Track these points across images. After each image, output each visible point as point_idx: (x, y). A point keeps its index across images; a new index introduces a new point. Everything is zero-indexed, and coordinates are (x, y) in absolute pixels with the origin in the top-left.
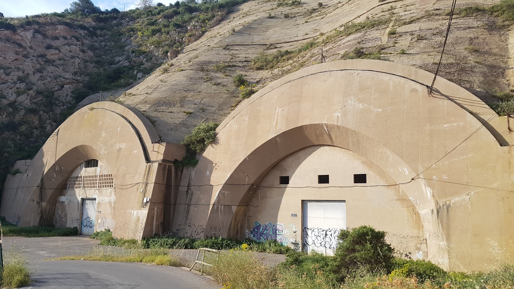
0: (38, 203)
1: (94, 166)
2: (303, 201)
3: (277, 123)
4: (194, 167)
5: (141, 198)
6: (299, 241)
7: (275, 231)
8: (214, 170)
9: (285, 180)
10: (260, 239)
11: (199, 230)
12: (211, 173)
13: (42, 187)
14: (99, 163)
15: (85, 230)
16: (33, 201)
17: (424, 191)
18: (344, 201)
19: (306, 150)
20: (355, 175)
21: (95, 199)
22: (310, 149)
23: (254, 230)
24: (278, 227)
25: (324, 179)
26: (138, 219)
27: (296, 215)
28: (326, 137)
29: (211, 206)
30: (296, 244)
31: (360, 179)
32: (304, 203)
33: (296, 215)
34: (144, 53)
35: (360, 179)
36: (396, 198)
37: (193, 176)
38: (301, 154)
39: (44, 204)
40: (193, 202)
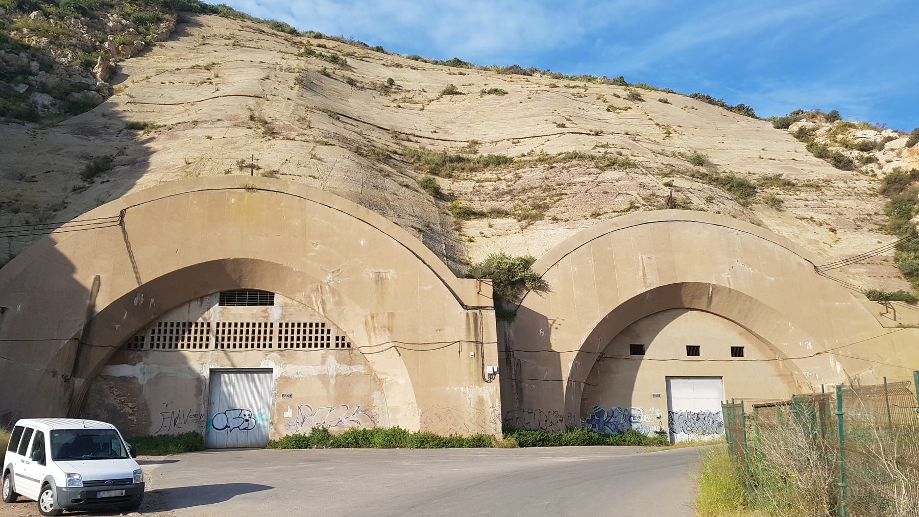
0: (66, 380)
1: (261, 304)
2: (668, 378)
3: (644, 274)
4: (510, 323)
5: (474, 366)
6: (666, 429)
7: (629, 418)
8: (553, 329)
9: (639, 350)
10: (604, 430)
11: (552, 418)
12: (548, 332)
13: (82, 342)
14: (277, 299)
15: (217, 437)
16: (55, 374)
17: (832, 364)
18: (721, 377)
19: (668, 313)
20: (699, 347)
21: (270, 371)
22: (674, 312)
23: (593, 417)
24: (633, 412)
25: (693, 351)
26: (481, 401)
27: (659, 396)
28: (705, 300)
29: (565, 384)
30: (662, 433)
31: (737, 352)
32: (668, 378)
33: (659, 396)
34: (29, 47)
35: (737, 352)
36: (776, 373)
37: (512, 336)
38: (661, 317)
39: (79, 382)
40: (525, 375)
